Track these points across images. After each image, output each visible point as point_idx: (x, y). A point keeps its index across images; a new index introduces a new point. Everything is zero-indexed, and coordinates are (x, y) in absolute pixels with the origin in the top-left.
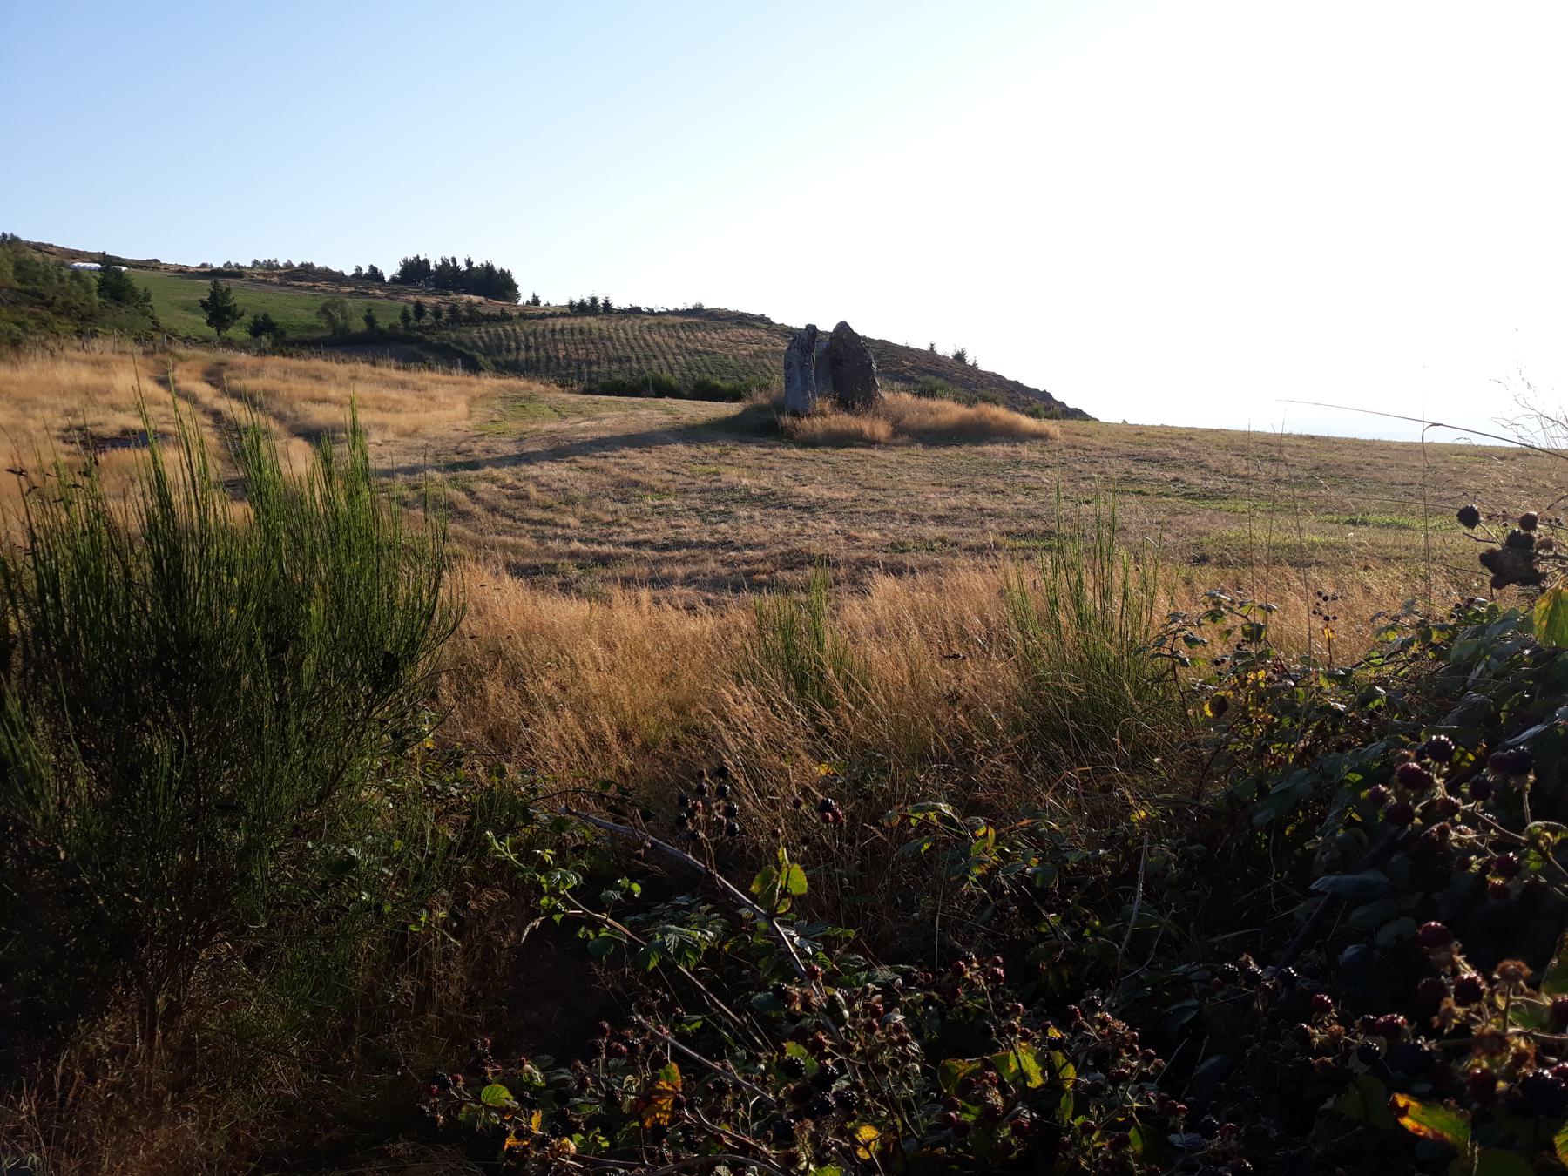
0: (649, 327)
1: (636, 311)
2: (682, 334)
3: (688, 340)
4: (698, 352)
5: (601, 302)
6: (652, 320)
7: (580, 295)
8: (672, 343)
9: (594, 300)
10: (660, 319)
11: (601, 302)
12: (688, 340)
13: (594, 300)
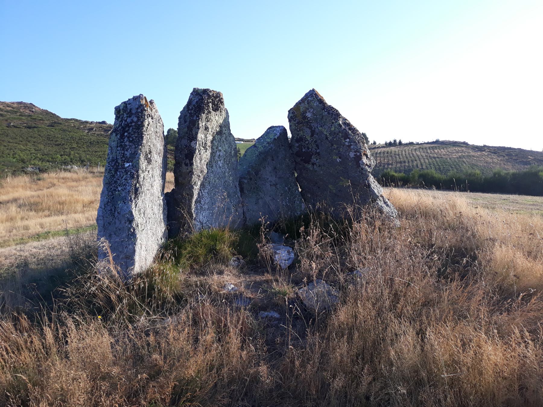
0: (415, 149)
1: (411, 144)
2: (429, 151)
3: (431, 153)
4: (435, 158)
5: (398, 141)
6: (418, 146)
7: (390, 139)
8: (423, 154)
9: (395, 141)
10: (421, 146)
11: (398, 141)
12: (431, 153)
13: (395, 141)
